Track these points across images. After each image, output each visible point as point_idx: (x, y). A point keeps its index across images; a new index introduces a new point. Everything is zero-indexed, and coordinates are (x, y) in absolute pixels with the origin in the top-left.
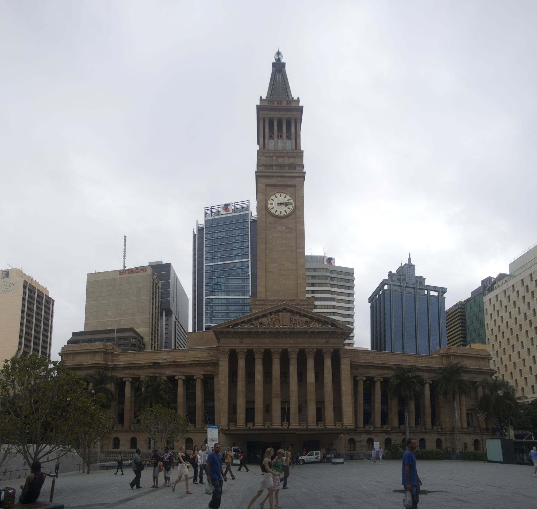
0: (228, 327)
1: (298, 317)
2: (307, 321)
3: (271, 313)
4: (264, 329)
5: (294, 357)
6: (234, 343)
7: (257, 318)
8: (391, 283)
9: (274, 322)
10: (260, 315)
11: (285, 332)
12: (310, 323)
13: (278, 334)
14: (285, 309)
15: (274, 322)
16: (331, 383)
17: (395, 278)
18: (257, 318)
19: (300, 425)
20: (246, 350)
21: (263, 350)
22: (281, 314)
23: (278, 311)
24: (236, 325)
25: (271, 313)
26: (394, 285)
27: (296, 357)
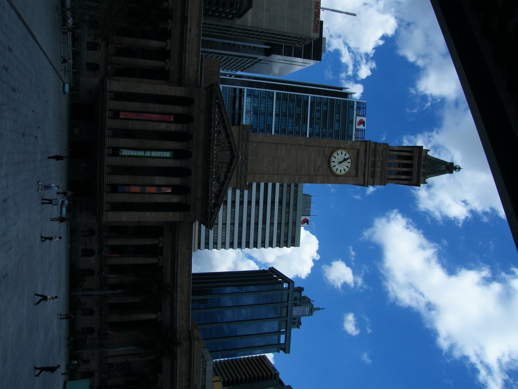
0: (217, 99)
1: (225, 170)
2: (220, 179)
3: (230, 143)
4: (214, 135)
7: (225, 128)
8: (291, 290)
14: (233, 157)
16: (153, 201)
17: (296, 295)
18: (225, 128)
19: (108, 166)
22: (228, 153)
24: (219, 107)
25: (230, 143)
26: (288, 294)
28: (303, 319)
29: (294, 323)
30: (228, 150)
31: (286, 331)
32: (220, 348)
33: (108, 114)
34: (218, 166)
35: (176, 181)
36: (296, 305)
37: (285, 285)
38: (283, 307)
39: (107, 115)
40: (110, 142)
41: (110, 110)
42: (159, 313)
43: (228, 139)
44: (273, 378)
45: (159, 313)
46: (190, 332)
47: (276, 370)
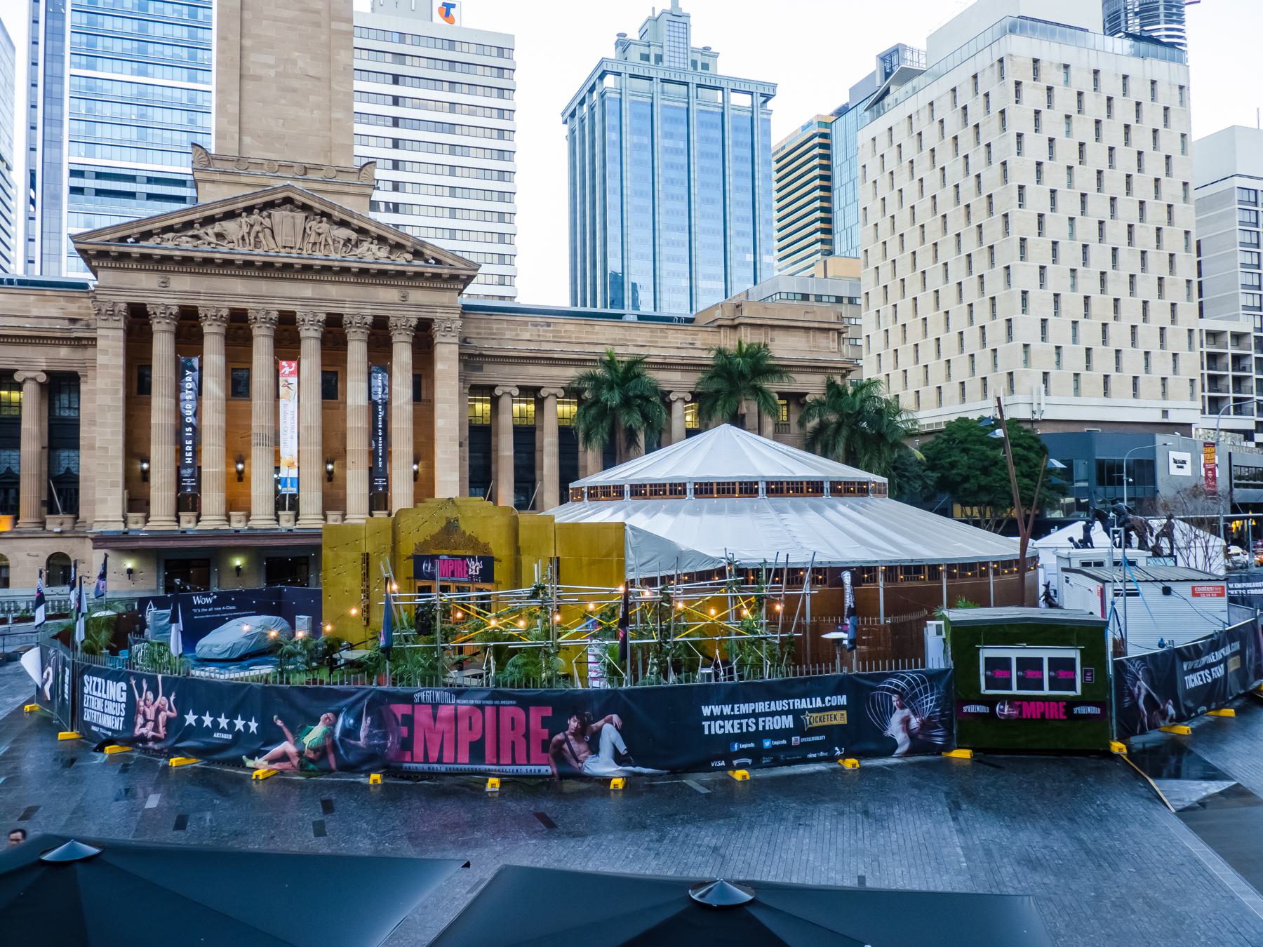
0: (123, 240)
1: (325, 226)
2: (349, 240)
3: (249, 210)
5: (312, 333)
6: (142, 286)
9: (257, 236)
10: (218, 211)
11: (287, 267)
12: (356, 246)
13: (267, 269)
14: (288, 201)
15: (257, 236)
16: (409, 408)
17: (634, 54)
20: (175, 310)
21: (225, 313)
22: (277, 214)
23: (271, 205)
24: (147, 235)
25: (249, 210)
26: (632, 76)
27: (319, 335)
28: (697, 42)
29: (705, 67)
30: (269, 216)
31: (722, 89)
32: (750, 257)
33: (187, 522)
34: (315, 244)
35: (357, 352)
36: (659, 58)
37: (609, 81)
38: (663, 92)
39: (191, 526)
40: (262, 516)
41: (178, 521)
42: (673, 397)
43: (240, 215)
44: (828, 131)
45: (673, 397)
46: (720, 326)
47: (810, 124)
